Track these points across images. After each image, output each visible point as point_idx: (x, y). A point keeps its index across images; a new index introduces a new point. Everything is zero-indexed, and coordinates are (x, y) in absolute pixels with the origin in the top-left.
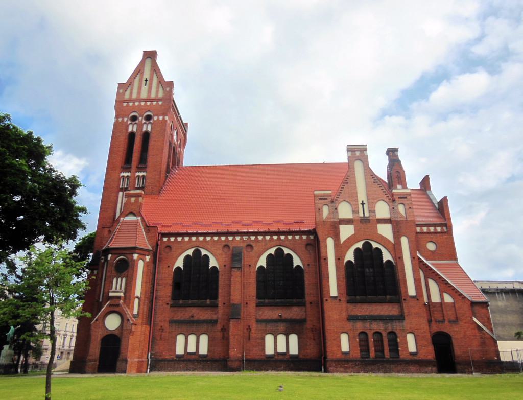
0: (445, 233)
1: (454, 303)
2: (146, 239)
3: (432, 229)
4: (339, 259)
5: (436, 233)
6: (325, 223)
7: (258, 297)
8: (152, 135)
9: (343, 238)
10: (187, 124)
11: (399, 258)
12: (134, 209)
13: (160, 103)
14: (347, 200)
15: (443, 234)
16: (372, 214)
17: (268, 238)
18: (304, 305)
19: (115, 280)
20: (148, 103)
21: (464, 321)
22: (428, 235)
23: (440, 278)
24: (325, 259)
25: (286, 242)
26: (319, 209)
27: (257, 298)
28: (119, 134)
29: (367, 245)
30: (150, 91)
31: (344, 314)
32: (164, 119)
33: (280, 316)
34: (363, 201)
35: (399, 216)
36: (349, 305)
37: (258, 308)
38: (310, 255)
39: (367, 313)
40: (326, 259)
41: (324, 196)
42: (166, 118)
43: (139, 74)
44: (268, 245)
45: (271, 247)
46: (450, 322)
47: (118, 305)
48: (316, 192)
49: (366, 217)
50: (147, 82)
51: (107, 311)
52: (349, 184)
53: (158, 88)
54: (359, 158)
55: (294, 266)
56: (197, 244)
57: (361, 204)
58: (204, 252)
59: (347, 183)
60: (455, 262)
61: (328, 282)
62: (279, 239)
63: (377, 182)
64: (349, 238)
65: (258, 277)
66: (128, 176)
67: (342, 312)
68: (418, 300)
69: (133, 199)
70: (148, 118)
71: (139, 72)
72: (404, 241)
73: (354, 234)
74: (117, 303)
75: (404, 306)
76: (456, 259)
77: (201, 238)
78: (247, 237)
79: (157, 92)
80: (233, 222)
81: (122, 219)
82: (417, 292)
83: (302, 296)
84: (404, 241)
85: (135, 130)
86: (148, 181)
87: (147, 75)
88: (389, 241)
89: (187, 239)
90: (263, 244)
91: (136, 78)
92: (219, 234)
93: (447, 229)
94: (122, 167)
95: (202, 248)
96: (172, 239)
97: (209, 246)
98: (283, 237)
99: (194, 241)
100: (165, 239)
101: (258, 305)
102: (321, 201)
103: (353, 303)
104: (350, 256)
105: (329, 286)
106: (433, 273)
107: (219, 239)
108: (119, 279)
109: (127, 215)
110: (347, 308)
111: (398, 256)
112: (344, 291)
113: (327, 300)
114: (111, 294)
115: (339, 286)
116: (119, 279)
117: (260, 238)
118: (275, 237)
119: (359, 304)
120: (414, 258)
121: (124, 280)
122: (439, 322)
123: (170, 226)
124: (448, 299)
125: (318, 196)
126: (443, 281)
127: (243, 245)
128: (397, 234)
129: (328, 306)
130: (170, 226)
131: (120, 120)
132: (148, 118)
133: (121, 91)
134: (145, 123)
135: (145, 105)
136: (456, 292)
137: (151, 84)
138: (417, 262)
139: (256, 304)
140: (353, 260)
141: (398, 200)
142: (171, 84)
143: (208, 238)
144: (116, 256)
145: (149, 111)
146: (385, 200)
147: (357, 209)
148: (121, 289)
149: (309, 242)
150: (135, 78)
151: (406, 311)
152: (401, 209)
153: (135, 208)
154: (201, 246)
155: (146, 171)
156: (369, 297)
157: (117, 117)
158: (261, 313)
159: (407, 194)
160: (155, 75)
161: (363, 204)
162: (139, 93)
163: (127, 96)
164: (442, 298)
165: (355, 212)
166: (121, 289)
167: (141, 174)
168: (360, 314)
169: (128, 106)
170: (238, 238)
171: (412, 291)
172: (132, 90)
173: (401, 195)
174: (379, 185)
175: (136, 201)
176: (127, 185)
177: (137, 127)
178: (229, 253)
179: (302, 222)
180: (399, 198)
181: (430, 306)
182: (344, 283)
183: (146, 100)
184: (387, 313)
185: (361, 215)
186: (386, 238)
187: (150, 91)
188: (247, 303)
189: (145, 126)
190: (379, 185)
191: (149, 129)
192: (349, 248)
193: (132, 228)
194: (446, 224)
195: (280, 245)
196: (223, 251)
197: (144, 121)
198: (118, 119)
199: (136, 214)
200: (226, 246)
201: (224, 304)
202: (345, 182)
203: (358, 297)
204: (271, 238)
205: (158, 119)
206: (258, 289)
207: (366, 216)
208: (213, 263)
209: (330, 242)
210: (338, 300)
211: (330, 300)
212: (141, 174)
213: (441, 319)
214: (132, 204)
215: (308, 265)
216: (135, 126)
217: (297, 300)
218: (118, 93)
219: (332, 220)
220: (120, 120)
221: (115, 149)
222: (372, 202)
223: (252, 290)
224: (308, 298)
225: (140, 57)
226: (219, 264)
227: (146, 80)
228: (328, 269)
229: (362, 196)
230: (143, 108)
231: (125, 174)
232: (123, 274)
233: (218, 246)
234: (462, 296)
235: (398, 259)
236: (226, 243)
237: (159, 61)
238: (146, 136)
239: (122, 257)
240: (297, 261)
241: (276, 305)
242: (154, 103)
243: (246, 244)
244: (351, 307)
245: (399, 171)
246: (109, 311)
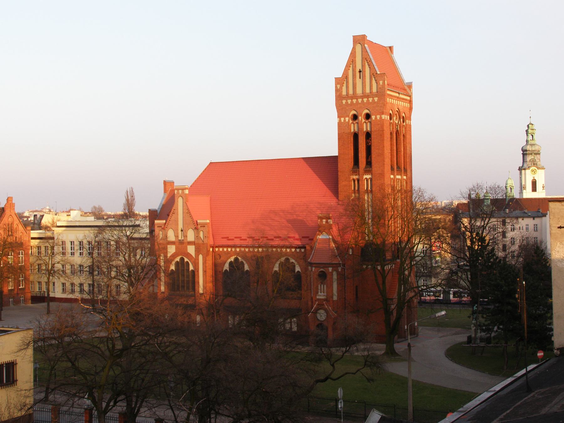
10: (410, 86)
50: (361, 73)
87: (359, 67)
131: (342, 119)
132: (368, 116)
133: (339, 86)
157: (339, 117)
160: (366, 64)
183: (362, 97)
218: (337, 90)
220: (342, 119)
238: (368, 135)
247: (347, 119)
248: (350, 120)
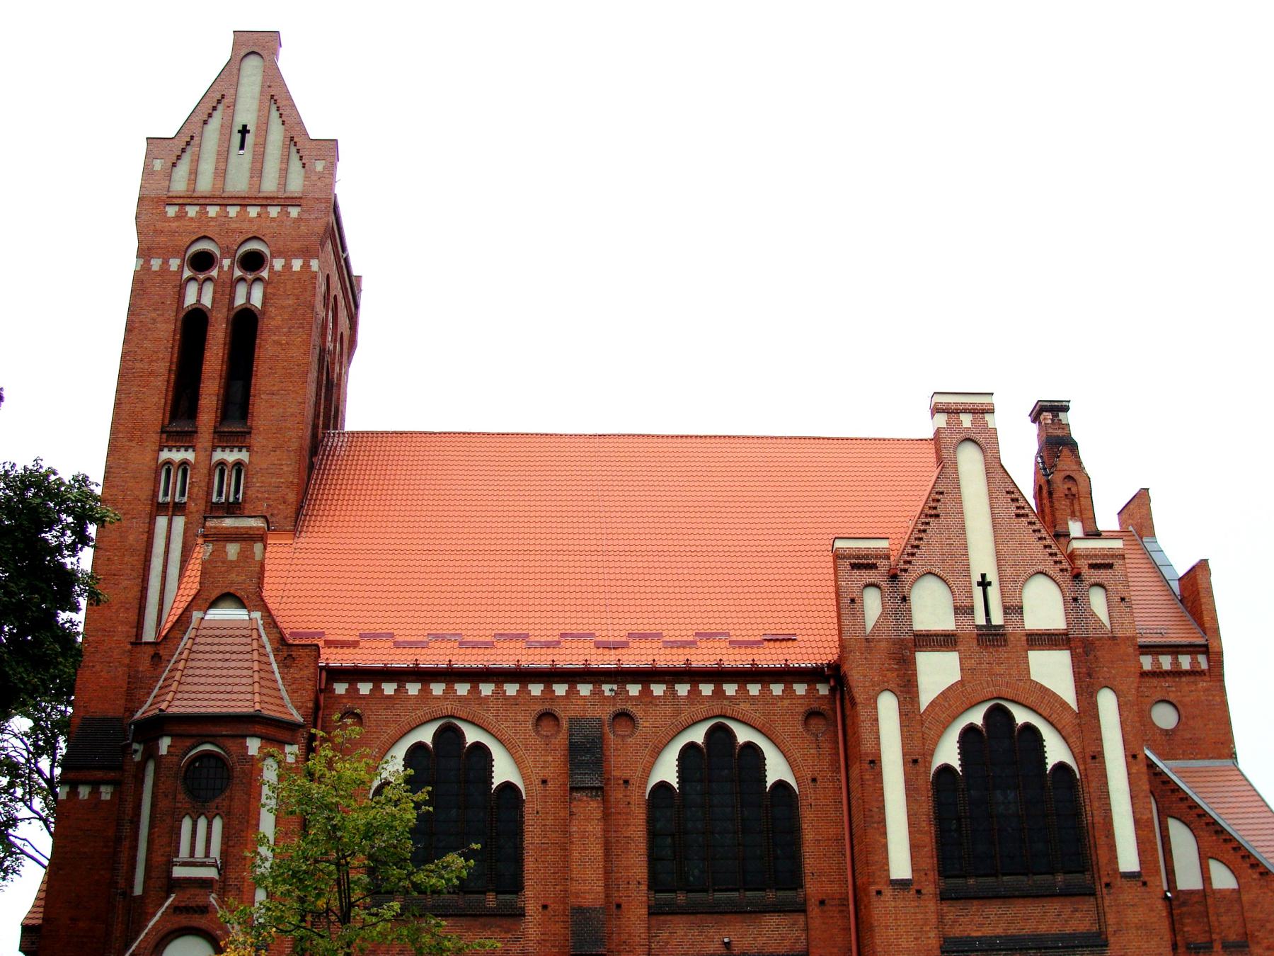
0: (1202, 673)
1: (1238, 891)
2: (282, 687)
3: (1166, 662)
4: (915, 761)
5: (1177, 673)
6: (872, 644)
7: (655, 884)
8: (264, 323)
9: (927, 695)
11: (1094, 758)
12: (238, 581)
13: (294, 212)
14: (936, 570)
15: (1198, 678)
16: (1014, 617)
17: (683, 690)
18: (802, 909)
19: (186, 824)
20: (253, 212)
21: (1265, 943)
22: (1155, 682)
23: (1199, 816)
24: (872, 762)
25: (744, 706)
26: (853, 601)
27: (650, 888)
28: (154, 315)
29: (998, 716)
30: (257, 171)
31: (932, 935)
32: (306, 266)
33: (727, 945)
34: (983, 576)
35: (1092, 626)
36: (945, 907)
37: (654, 920)
38: (818, 747)
39: (999, 931)
40: (875, 762)
41: (867, 557)
42: (315, 264)
43: (220, 107)
44: (684, 717)
45: (695, 723)
46: (1225, 946)
47: (205, 909)
48: (839, 544)
49: (996, 626)
50: (250, 138)
51: (170, 926)
52: (942, 519)
53: (286, 160)
54: (973, 436)
55: (768, 785)
56: (448, 707)
57: (979, 584)
58: (472, 736)
59: (937, 516)
60: (1228, 762)
61: (884, 834)
62: (719, 693)
63: (1027, 515)
64: (944, 694)
65: (651, 820)
66: (184, 463)
67: (928, 928)
68: (1145, 884)
69: (233, 550)
70: (253, 262)
71: (219, 102)
72: (1107, 703)
73: (961, 683)
74: (200, 901)
75: (1107, 903)
76: (1233, 756)
77: (462, 689)
78: (615, 687)
79: (284, 172)
80: (562, 635)
81: (196, 615)
82: (1141, 862)
83: (792, 878)
84: (1107, 703)
85: (207, 301)
86: (257, 482)
88: (1064, 704)
89: (413, 689)
90: (669, 710)
91: (211, 120)
92: (522, 676)
93: (1209, 661)
94: (162, 432)
95: (465, 720)
96: (365, 688)
97: (490, 716)
98: (730, 689)
99: (437, 698)
100: (340, 688)
101: (655, 911)
102: (856, 572)
103: (957, 899)
104: (948, 753)
105: (885, 846)
106: (1182, 799)
107: (524, 690)
108: (202, 823)
109: (214, 604)
110: (941, 917)
111: (1095, 757)
112: (929, 863)
113: (879, 893)
114: (178, 872)
115: (914, 847)
116: (202, 823)
117: (658, 690)
118: (707, 689)
119: (974, 906)
120: (1134, 757)
121: (218, 824)
122: (1198, 948)
123: (354, 644)
124: (1223, 878)
125: (850, 556)
126: (1207, 824)
127: (606, 713)
128: (1086, 684)
129: (885, 910)
130: (354, 644)
131: (156, 264)
132: (253, 262)
133: (158, 165)
134: (242, 279)
135: (242, 217)
136: (1243, 857)
137: (262, 145)
138: (1144, 769)
139: (649, 907)
140: (955, 763)
141: (1090, 575)
142: (329, 148)
143: (487, 689)
144: (188, 743)
145: (255, 238)
146: (1051, 573)
147: (967, 603)
148: (207, 854)
149: (815, 705)
150: (205, 122)
151: (1111, 919)
152: (1098, 602)
153: (240, 579)
154: (464, 715)
155: (249, 449)
156: (1005, 878)
157: (144, 253)
158: (664, 935)
159: (1113, 556)
160: (275, 114)
161: (984, 584)
162: (221, 173)
163: (179, 184)
164: (1206, 876)
165: (963, 610)
166: (207, 854)
167: (231, 456)
168: (979, 934)
170: (585, 690)
171: (1128, 858)
172: (196, 162)
173: (1095, 556)
174: (1030, 523)
175: (245, 556)
176: (183, 494)
177: (215, 292)
178: (561, 740)
179: (790, 639)
180: (1093, 566)
181: (1176, 903)
182: (929, 840)
183: (243, 202)
184: (1055, 929)
185: (980, 619)
186: (1054, 694)
187: (257, 171)
188: (619, 906)
189: (241, 291)
190: (1030, 523)
191: (257, 299)
192: (946, 726)
193: (235, 648)
194: (1206, 646)
195: (725, 717)
196: (538, 733)
197: (238, 273)
198: (147, 262)
199: (246, 601)
200: (546, 716)
201: (545, 907)
202: (931, 512)
203: (971, 881)
204: (694, 692)
205: (287, 267)
206: (653, 859)
207: (994, 623)
208: (503, 770)
209: (888, 707)
210: (913, 892)
211: (888, 892)
212: (231, 456)
213: (1201, 939)
214: (231, 566)
215: (814, 780)
216: (209, 290)
217: (780, 893)
219: (893, 635)
220: (156, 264)
221: (138, 365)
222: (1013, 584)
223: (636, 864)
224: (812, 888)
225: (223, 53)
226: (524, 777)
227: (244, 131)
228: (882, 795)
229: (982, 560)
230: (234, 226)
231: (177, 456)
232: (213, 804)
233: (520, 718)
234: (1262, 871)
235: (1089, 760)
236: (547, 706)
237: (287, 63)
239: (208, 747)
240: (776, 769)
241: (715, 910)
242: (274, 212)
243: (610, 710)
244: (951, 910)
245: (1072, 474)
246: (176, 926)
247: (174, 264)
248: (186, 268)
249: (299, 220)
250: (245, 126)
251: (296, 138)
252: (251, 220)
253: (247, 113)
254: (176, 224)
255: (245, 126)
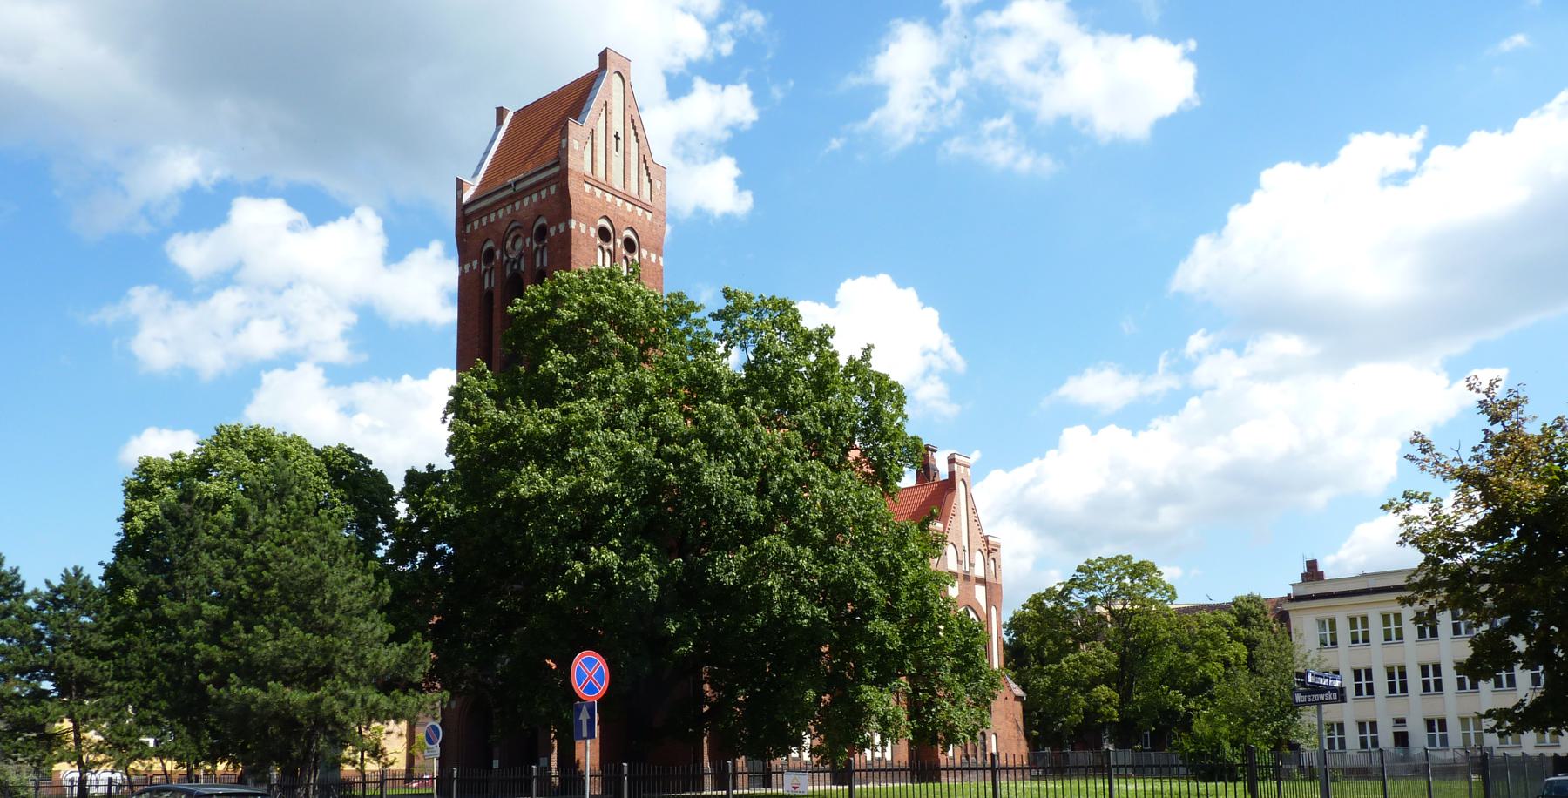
13: (649, 216)
50: (621, 143)
165: (959, 562)
169: (592, 194)
247: (593, 232)
249: (651, 224)
250: (617, 133)
251: (644, 161)
252: (629, 213)
253: (617, 126)
254: (590, 199)
255: (617, 133)
